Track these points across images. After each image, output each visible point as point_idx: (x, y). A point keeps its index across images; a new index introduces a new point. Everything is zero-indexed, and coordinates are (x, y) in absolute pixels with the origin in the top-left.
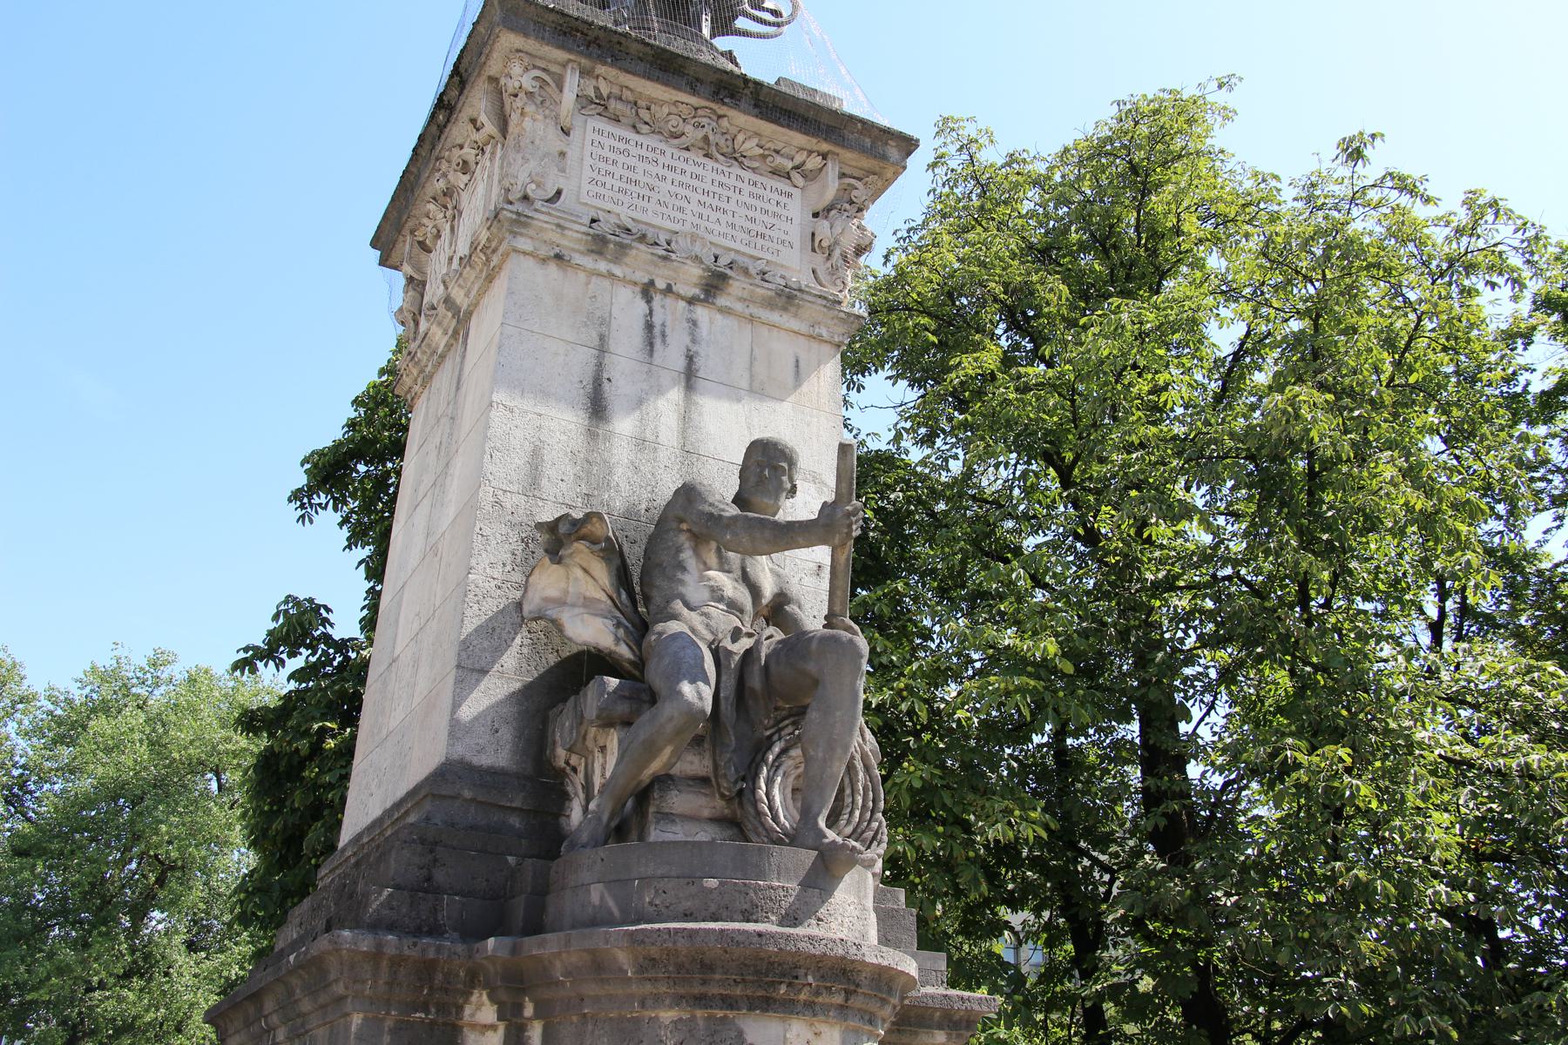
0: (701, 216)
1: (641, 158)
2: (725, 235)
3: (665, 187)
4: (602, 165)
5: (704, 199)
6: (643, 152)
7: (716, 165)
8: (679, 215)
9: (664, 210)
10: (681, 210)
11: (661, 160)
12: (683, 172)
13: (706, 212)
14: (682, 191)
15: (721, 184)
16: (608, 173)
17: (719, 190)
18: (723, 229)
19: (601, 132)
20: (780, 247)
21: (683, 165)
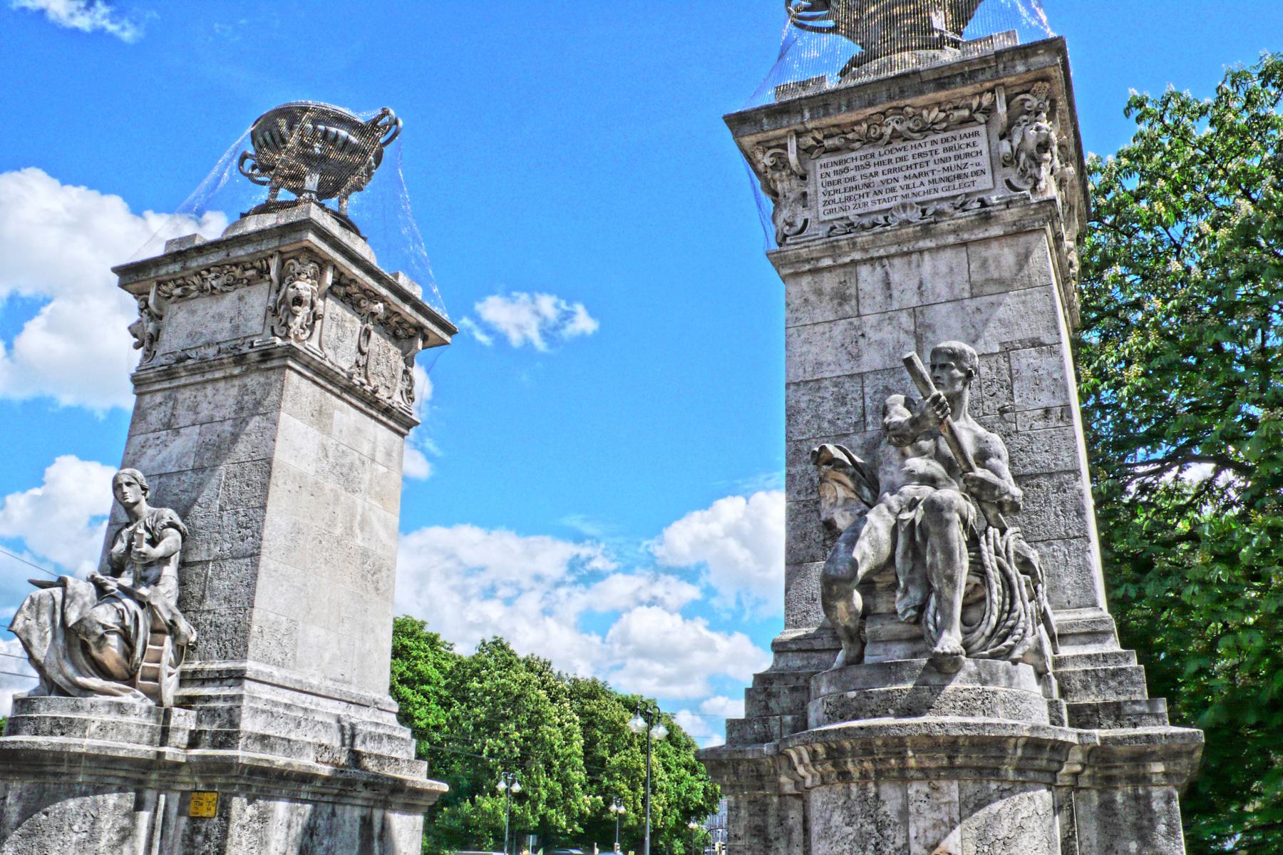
1: (857, 168)
2: (929, 192)
3: (877, 180)
4: (829, 189)
6: (859, 163)
7: (913, 143)
8: (891, 195)
9: (880, 197)
10: (893, 190)
11: (872, 161)
12: (890, 161)
13: (910, 182)
14: (890, 176)
17: (918, 161)
18: (927, 187)
19: (826, 166)
20: (975, 178)
21: (891, 156)
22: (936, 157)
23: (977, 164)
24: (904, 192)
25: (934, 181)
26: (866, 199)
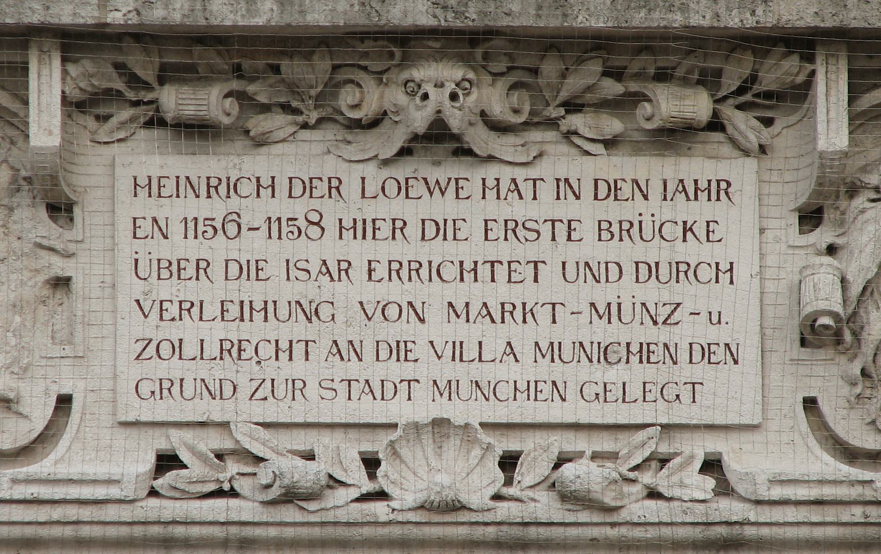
0: (458, 352)
4: (167, 289)
5: (459, 293)
6: (281, 207)
7: (492, 172)
8: (396, 370)
9: (353, 369)
15: (512, 228)
16: (186, 308)
17: (504, 250)
22: (574, 253)
23: (716, 319)
24: (448, 370)
25: (554, 351)
26: (298, 368)
